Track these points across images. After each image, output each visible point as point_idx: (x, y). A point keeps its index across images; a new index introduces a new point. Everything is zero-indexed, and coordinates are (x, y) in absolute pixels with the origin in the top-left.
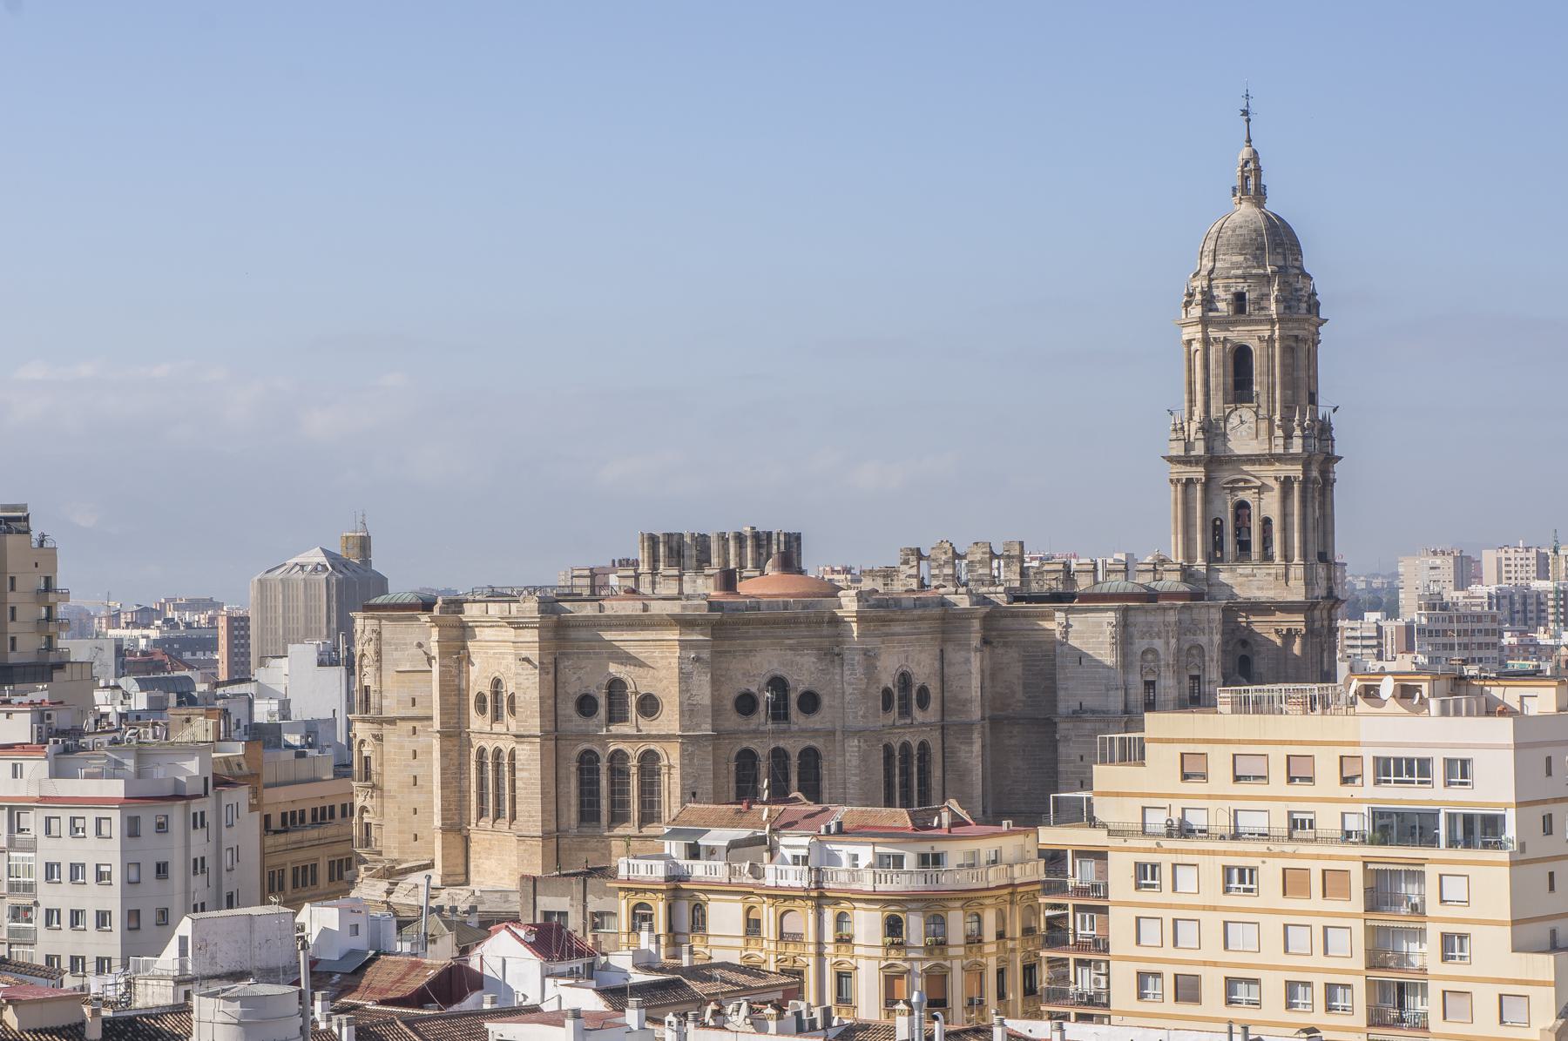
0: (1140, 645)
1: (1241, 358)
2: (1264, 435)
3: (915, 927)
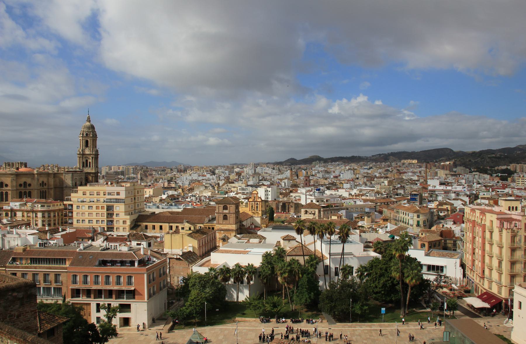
0: (75, 178)
2: (90, 151)
3: (46, 215)
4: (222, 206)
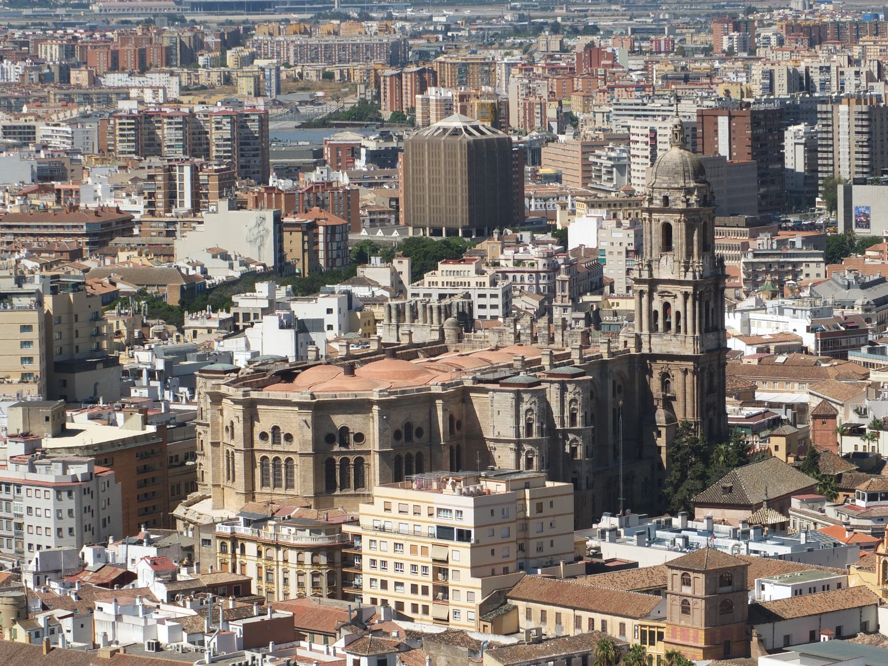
1: (667, 229)
4: (679, 573)
